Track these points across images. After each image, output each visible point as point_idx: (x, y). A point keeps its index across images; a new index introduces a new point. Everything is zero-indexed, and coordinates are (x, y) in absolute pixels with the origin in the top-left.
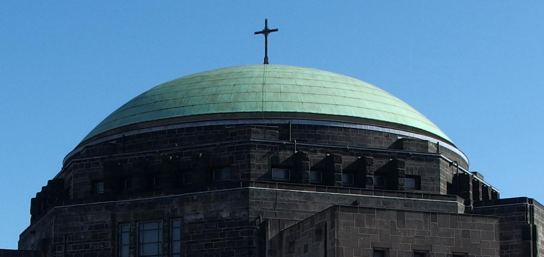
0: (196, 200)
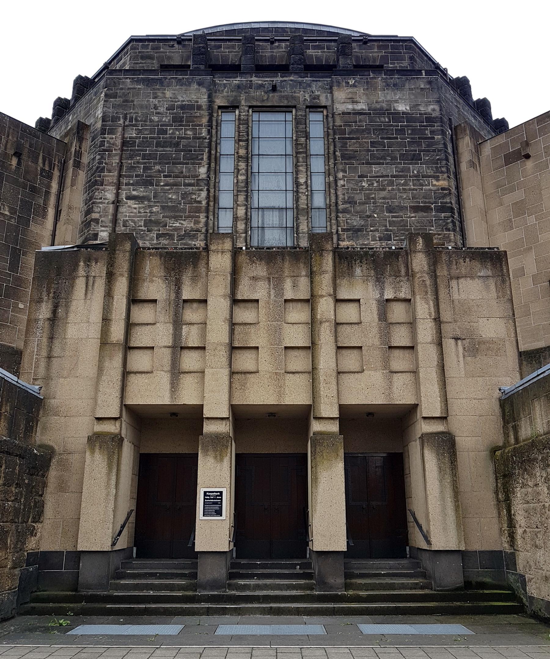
0: (354, 86)
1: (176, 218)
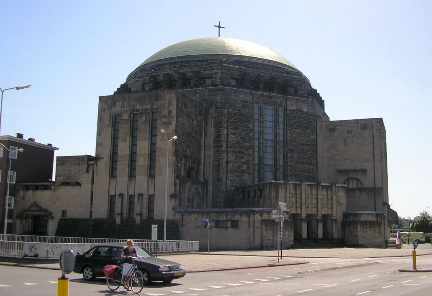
0: (292, 100)
1: (245, 142)
